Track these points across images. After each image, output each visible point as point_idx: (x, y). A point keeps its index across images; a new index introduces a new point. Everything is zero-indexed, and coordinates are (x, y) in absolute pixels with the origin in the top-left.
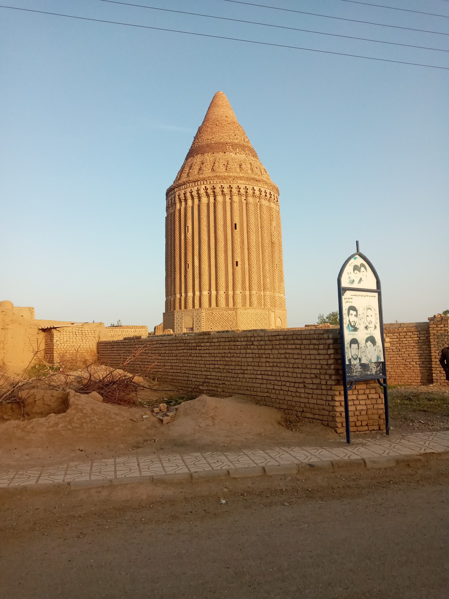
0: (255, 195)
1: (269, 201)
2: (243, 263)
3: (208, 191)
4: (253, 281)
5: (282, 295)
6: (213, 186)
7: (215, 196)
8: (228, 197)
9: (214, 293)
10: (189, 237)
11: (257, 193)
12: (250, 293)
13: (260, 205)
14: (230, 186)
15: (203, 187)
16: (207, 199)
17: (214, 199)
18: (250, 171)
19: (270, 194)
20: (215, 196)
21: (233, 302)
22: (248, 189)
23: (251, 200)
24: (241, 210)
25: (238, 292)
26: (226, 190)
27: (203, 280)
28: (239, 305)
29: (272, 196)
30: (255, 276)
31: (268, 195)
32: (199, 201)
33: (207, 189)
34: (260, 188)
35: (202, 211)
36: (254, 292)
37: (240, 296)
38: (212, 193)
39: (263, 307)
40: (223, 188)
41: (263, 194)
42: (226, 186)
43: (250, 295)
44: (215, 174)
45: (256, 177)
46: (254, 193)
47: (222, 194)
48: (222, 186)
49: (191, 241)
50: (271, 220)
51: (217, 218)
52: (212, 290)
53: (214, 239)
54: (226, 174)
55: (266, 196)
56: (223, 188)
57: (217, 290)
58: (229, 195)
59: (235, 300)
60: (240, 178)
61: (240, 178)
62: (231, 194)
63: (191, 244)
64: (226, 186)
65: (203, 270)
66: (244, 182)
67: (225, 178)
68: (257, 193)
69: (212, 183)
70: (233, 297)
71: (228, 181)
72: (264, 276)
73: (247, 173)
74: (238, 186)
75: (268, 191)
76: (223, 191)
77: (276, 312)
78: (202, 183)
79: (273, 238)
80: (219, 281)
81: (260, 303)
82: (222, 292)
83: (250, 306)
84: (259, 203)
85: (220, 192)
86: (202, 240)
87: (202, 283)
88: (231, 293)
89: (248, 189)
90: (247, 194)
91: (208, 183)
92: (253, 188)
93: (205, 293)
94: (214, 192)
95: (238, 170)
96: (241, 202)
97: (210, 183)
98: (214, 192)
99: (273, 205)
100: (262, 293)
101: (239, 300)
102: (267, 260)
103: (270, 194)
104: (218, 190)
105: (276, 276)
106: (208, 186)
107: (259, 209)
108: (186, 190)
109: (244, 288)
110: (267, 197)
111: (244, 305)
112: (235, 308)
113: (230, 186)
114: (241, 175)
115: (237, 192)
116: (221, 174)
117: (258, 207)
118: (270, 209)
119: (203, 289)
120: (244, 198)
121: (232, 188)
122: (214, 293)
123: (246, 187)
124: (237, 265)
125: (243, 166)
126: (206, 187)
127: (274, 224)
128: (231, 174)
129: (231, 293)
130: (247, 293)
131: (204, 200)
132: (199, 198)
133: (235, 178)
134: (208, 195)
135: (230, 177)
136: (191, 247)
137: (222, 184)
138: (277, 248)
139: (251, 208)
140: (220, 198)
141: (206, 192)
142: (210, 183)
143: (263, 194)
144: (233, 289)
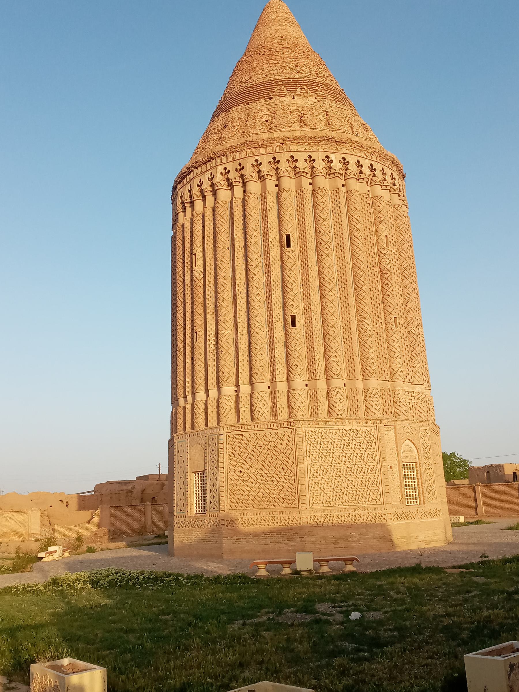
0: (333, 171)
1: (370, 183)
2: (309, 319)
3: (230, 176)
4: (333, 358)
5: (418, 388)
6: (240, 164)
7: (244, 185)
8: (271, 184)
9: (245, 389)
10: (197, 275)
11: (337, 166)
12: (328, 385)
13: (347, 193)
14: (274, 158)
15: (220, 169)
16: (229, 193)
17: (245, 191)
18: (322, 126)
19: (372, 169)
20: (244, 185)
21: (289, 409)
22: (314, 160)
23: (322, 182)
24: (300, 206)
25: (299, 384)
26: (265, 169)
27: (222, 363)
28: (303, 411)
29: (378, 173)
30: (338, 348)
31: (366, 170)
32: (215, 199)
33: (229, 172)
34: (343, 156)
35: (218, 218)
36: (337, 383)
37: (305, 394)
38: (238, 179)
39: (363, 416)
40: (261, 164)
41: (353, 168)
42: (265, 160)
43: (328, 391)
44: (243, 140)
45: (334, 135)
46: (330, 168)
47: (260, 178)
48: (257, 161)
49: (201, 284)
50: (378, 224)
51: (249, 228)
52: (240, 383)
53: (243, 273)
54: (266, 136)
55: (361, 172)
56: (261, 164)
57: (252, 383)
58: (274, 178)
59: (292, 404)
60: (297, 140)
61: (297, 140)
62: (277, 174)
63: (201, 290)
64: (265, 160)
65: (221, 341)
66: (307, 147)
67: (261, 145)
68: (337, 166)
69: (237, 156)
70: (288, 396)
71: (270, 149)
72: (363, 345)
73: (314, 128)
74: (292, 157)
75: (366, 163)
76: (259, 171)
77: (399, 425)
78: (219, 161)
79: (382, 262)
80: (254, 362)
81: (353, 408)
82: (262, 387)
83: (330, 414)
84: (344, 189)
85: (255, 175)
86: (220, 278)
87: (222, 370)
88: (282, 387)
89: (314, 160)
90: (314, 170)
91: (230, 159)
92: (327, 157)
93: (229, 390)
94: (242, 176)
95: (296, 126)
96: (300, 189)
97: (234, 159)
98: (242, 176)
99: (378, 190)
100: (360, 385)
101: (301, 401)
102: (368, 310)
103: (372, 169)
104: (249, 171)
105: (398, 348)
106: (230, 167)
107: (343, 200)
108: (191, 183)
109: (312, 376)
110: (363, 176)
111: (314, 412)
112: (291, 422)
113: (274, 158)
114: (298, 133)
115: (289, 170)
116: (255, 138)
117: (342, 195)
118: (374, 200)
119: (222, 383)
120: (306, 181)
121: (278, 162)
122: (245, 389)
123: (310, 157)
124: (294, 324)
125: (308, 118)
126: (225, 168)
127: (384, 231)
128: (276, 135)
129: (282, 387)
130: (322, 385)
131: (224, 195)
132: (215, 193)
133: (284, 142)
134: (231, 186)
135: (274, 140)
136: (201, 296)
137: (257, 158)
138: (395, 282)
139: (326, 200)
140: (254, 187)
141: (228, 180)
142: (234, 159)
143: (353, 168)
144: (288, 378)
